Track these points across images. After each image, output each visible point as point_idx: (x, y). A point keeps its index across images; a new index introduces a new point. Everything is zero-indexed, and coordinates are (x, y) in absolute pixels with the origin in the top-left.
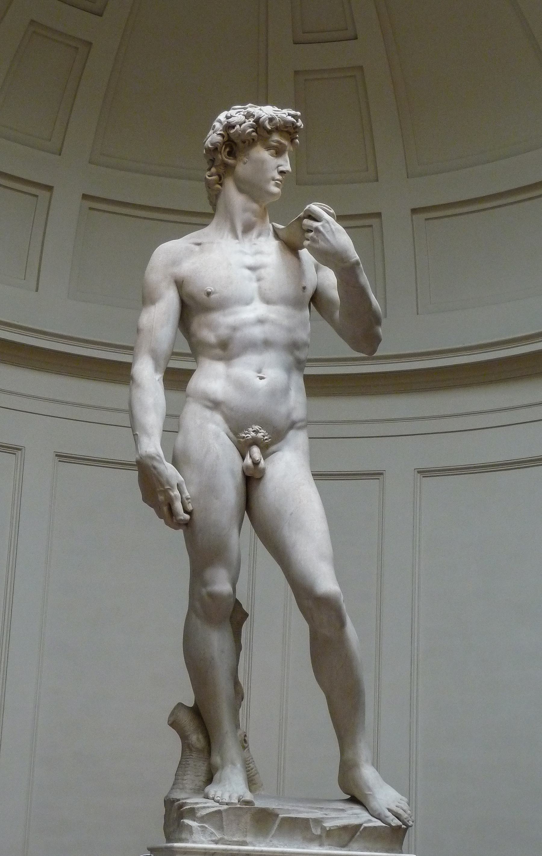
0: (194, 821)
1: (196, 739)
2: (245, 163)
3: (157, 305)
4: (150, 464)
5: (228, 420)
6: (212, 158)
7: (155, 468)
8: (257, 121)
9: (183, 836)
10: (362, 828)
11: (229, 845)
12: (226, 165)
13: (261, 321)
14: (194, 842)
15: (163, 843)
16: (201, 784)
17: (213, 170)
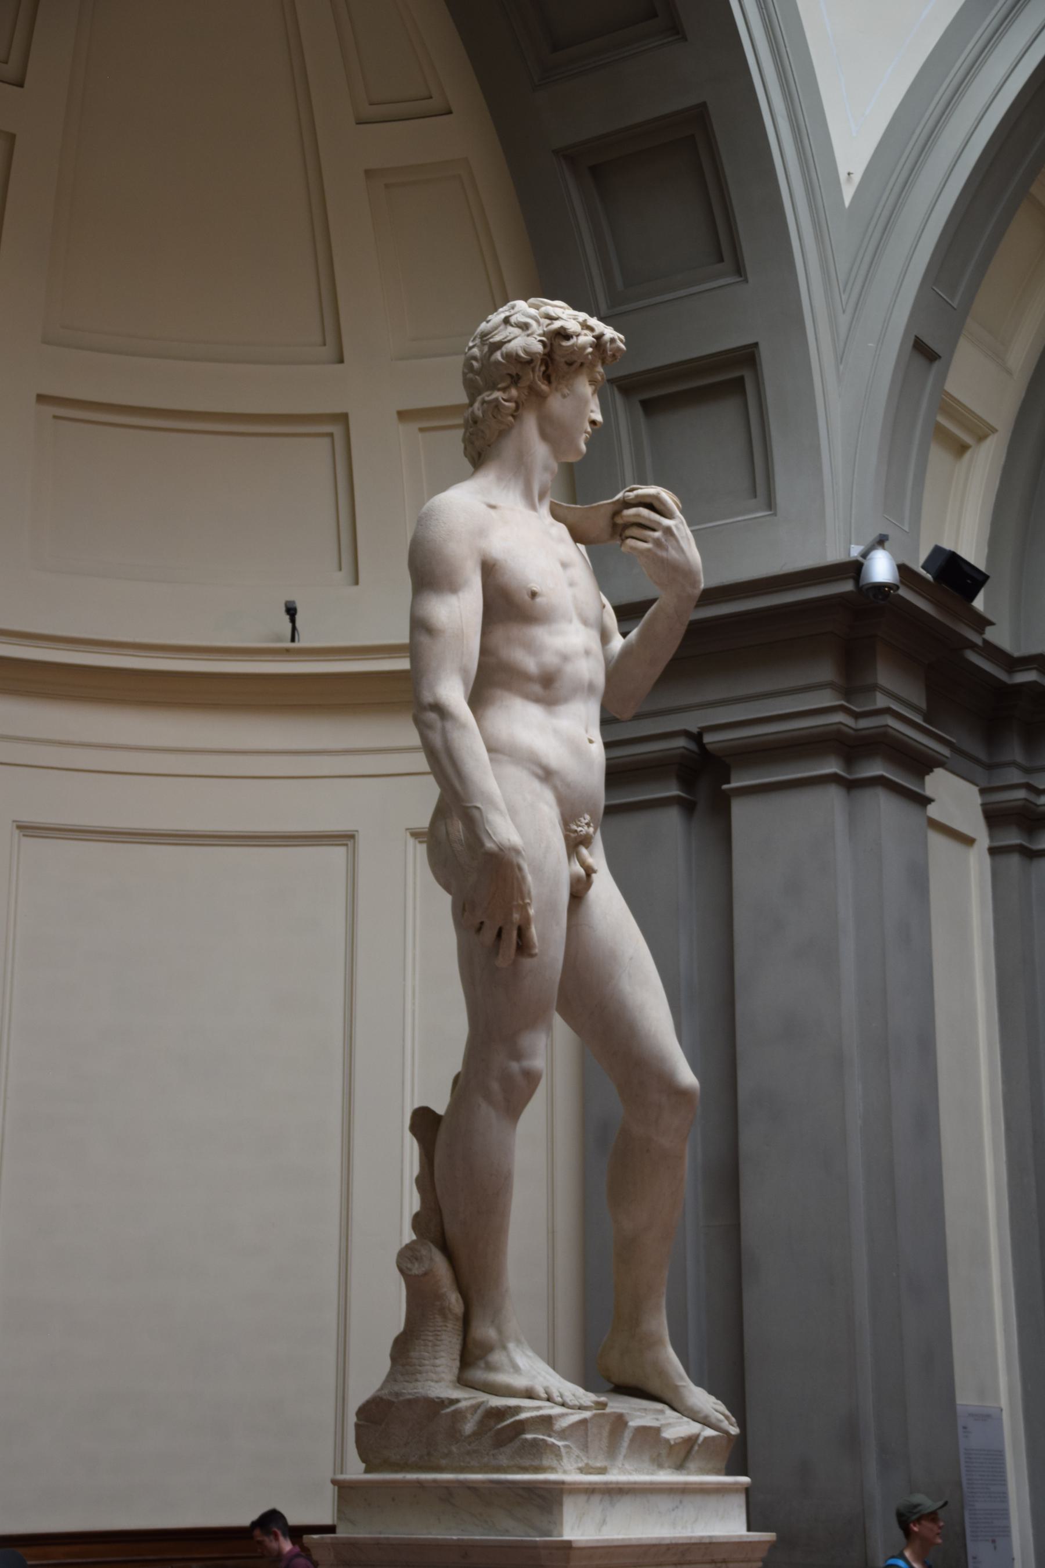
0: (550, 1436)
1: (454, 1300)
2: (564, 396)
3: (461, 594)
4: (515, 862)
5: (562, 801)
6: (514, 373)
7: (520, 869)
8: (599, 337)
9: (546, 1462)
10: (701, 1439)
11: (591, 1473)
12: (532, 390)
13: (587, 653)
14: (565, 1472)
15: (355, 1470)
16: (456, 1371)
17: (514, 392)
